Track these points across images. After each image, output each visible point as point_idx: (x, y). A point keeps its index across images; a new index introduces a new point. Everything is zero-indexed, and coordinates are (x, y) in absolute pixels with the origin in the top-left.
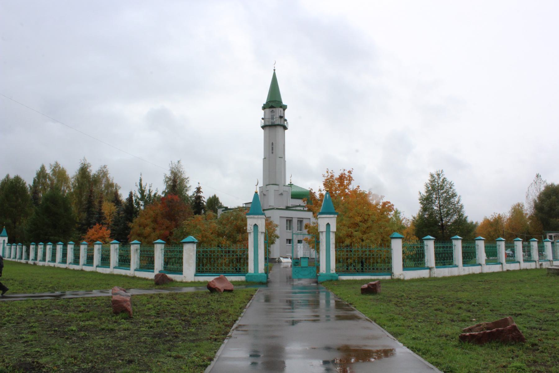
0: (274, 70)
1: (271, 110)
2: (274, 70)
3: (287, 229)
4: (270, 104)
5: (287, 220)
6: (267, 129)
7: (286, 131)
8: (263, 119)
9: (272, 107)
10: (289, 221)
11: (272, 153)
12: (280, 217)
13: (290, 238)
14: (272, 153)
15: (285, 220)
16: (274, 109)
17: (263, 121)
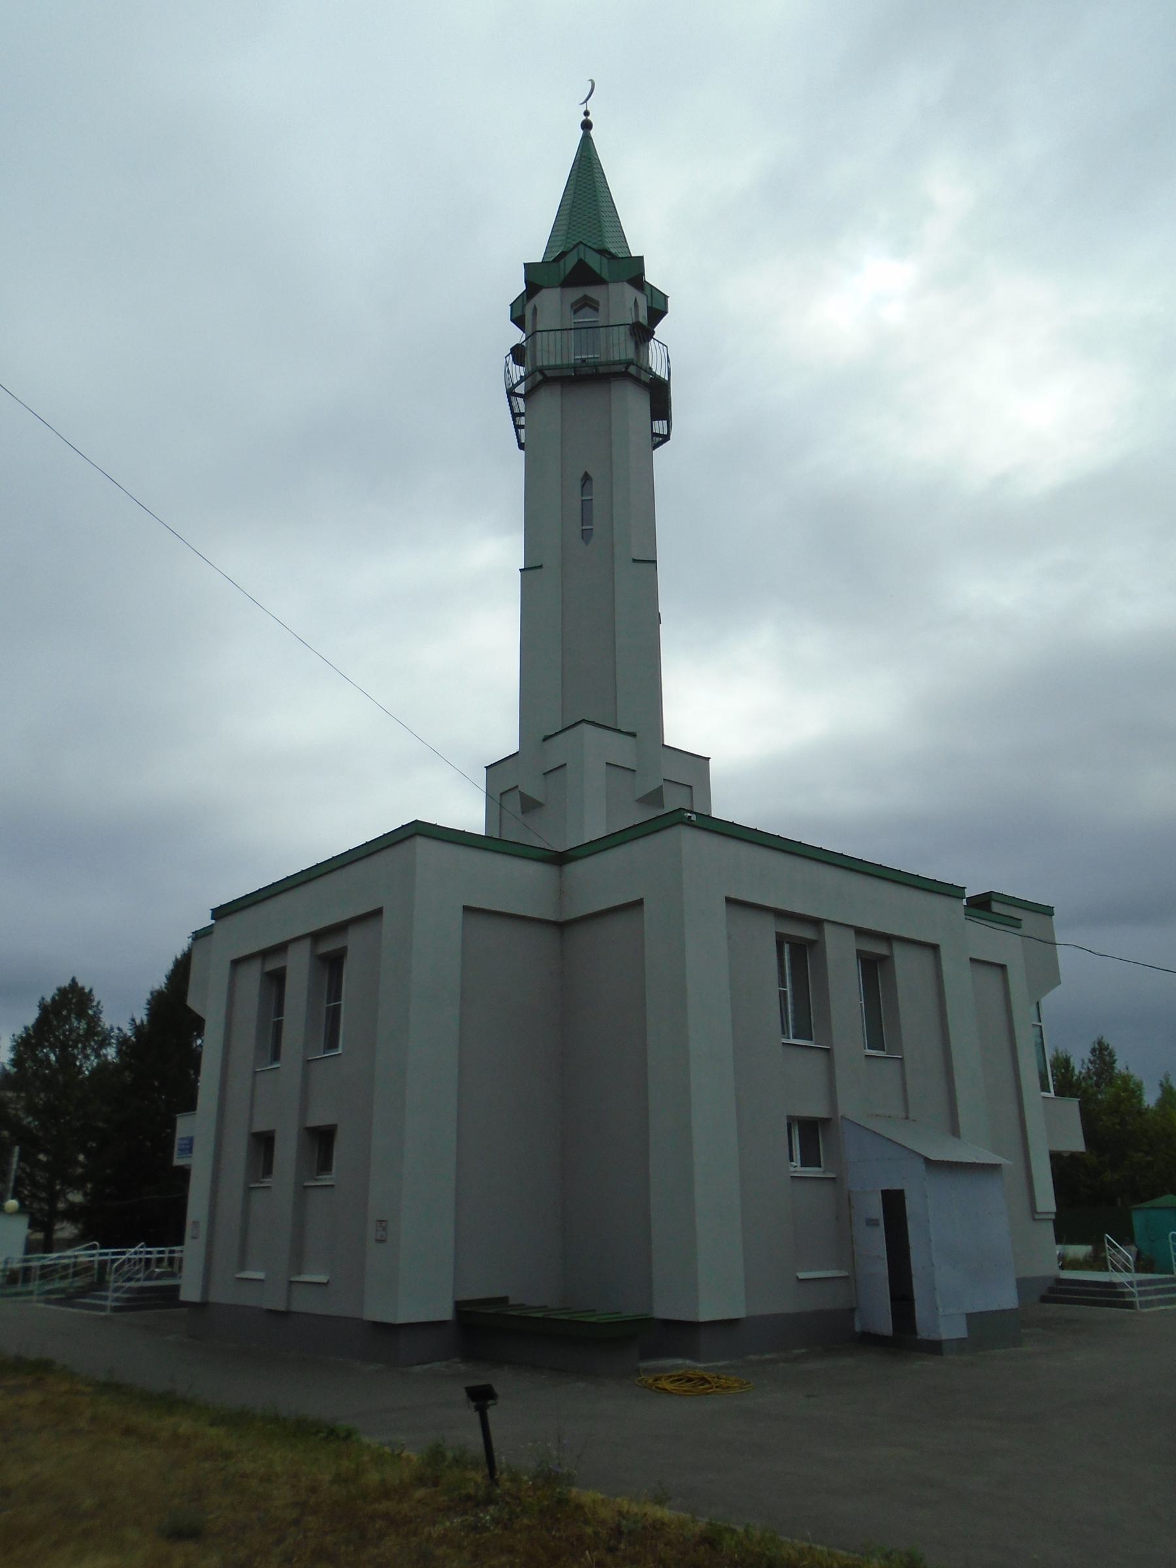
0: (587, 126)
1: (576, 293)
2: (587, 126)
3: (784, 1031)
4: (570, 262)
5: (781, 940)
6: (550, 400)
7: (656, 453)
8: (518, 354)
9: (582, 276)
10: (800, 948)
11: (586, 535)
12: (729, 901)
13: (817, 1110)
14: (586, 535)
15: (766, 932)
16: (593, 292)
17: (518, 372)
